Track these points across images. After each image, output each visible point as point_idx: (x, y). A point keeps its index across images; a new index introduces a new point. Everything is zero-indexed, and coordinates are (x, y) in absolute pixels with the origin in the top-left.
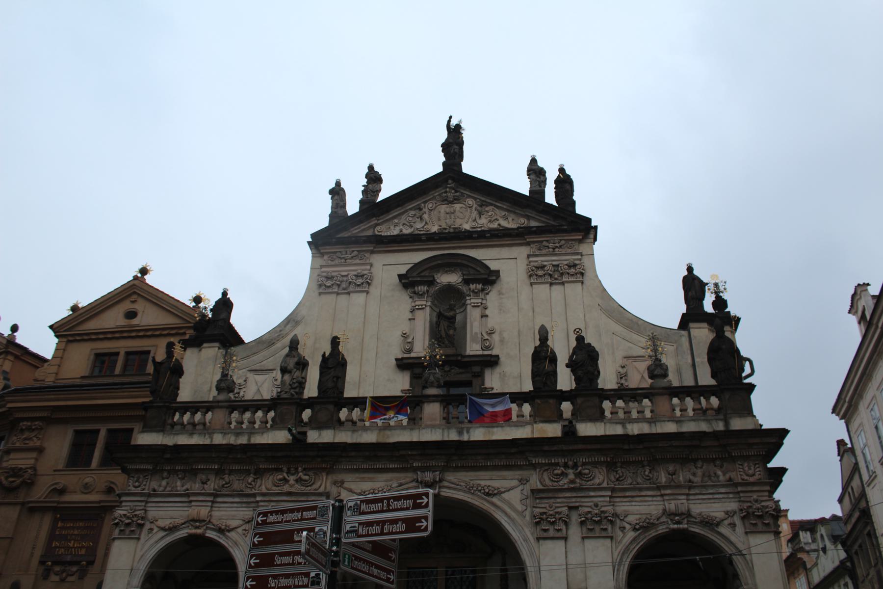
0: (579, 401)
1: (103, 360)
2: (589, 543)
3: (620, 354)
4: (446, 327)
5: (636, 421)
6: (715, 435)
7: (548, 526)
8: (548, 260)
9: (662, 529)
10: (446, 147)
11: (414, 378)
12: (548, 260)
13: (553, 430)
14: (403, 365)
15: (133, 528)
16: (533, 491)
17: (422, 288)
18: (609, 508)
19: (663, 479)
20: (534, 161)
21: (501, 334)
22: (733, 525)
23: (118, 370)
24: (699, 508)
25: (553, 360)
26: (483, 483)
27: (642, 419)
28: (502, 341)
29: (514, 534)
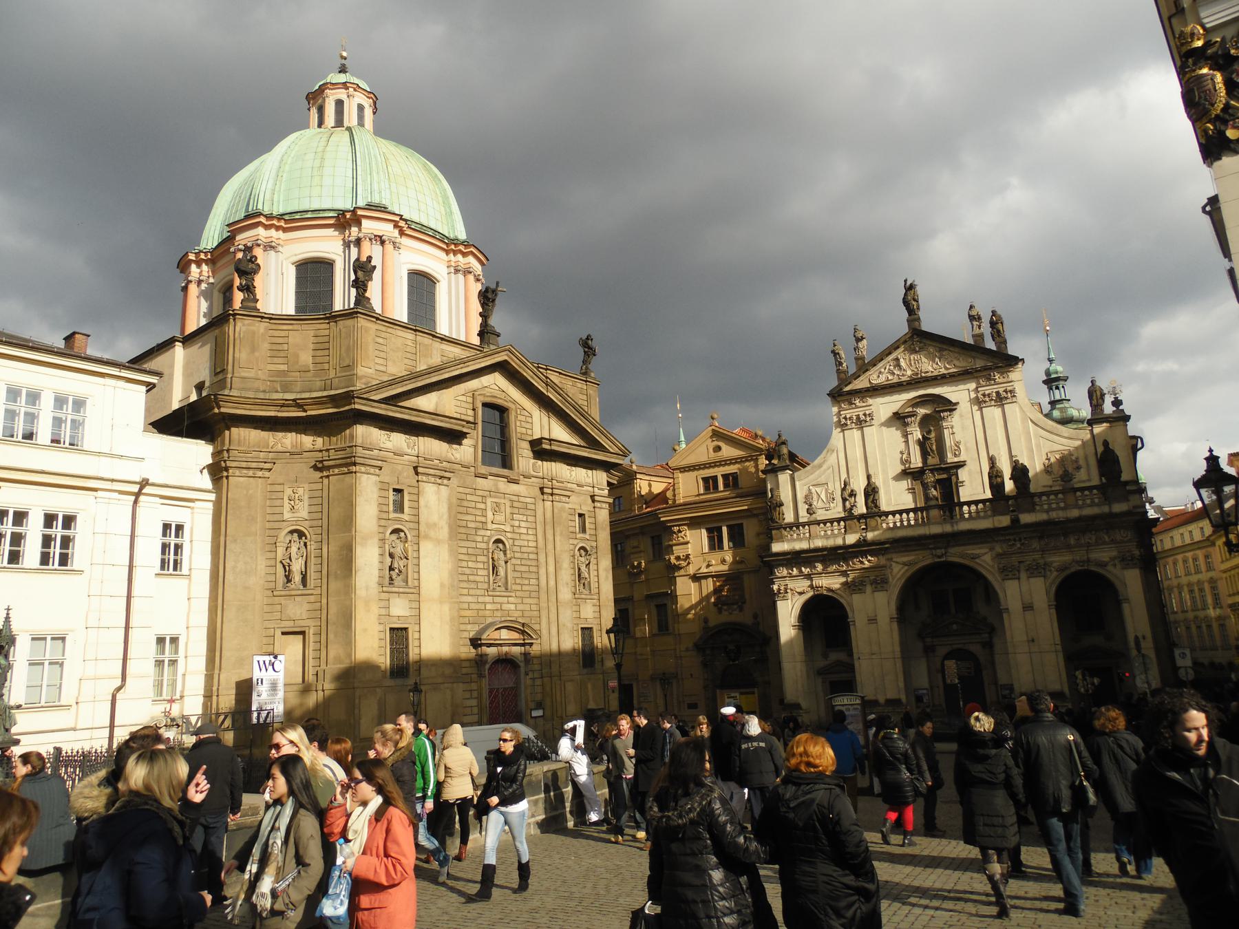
1: (710, 483)
2: (1033, 580)
4: (932, 445)
5: (1054, 510)
7: (1008, 572)
9: (1073, 570)
10: (906, 303)
13: (1005, 521)
14: (906, 473)
16: (999, 555)
18: (1041, 562)
19: (1072, 542)
20: (971, 307)
23: (721, 487)
25: (1002, 477)
27: (1060, 509)
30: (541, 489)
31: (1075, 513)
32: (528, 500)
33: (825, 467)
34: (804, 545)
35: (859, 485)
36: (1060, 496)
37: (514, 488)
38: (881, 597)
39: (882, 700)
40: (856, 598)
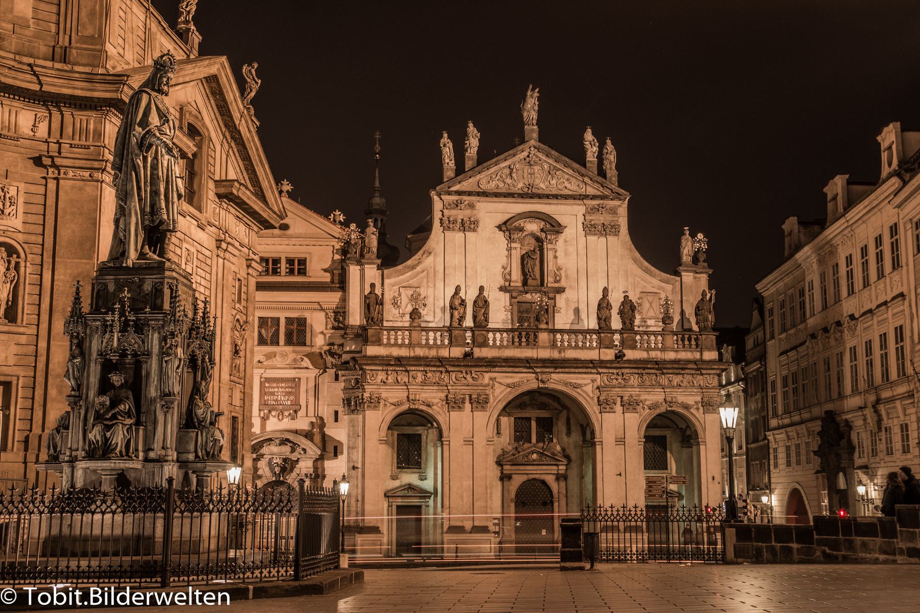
0: (625, 335)
3: (638, 290)
6: (695, 362)
8: (599, 219)
9: (663, 409)
11: (512, 297)
12: (599, 219)
15: (375, 402)
17: (515, 236)
21: (566, 271)
22: (698, 409)
23: (283, 273)
24: (681, 399)
26: (573, 381)
28: (567, 276)
29: (589, 409)
30: (219, 241)
31: (671, 356)
32: (208, 253)
33: (419, 269)
34: (404, 352)
35: (470, 295)
36: (660, 338)
37: (200, 235)
38: (481, 417)
39: (468, 525)
40: (454, 414)
